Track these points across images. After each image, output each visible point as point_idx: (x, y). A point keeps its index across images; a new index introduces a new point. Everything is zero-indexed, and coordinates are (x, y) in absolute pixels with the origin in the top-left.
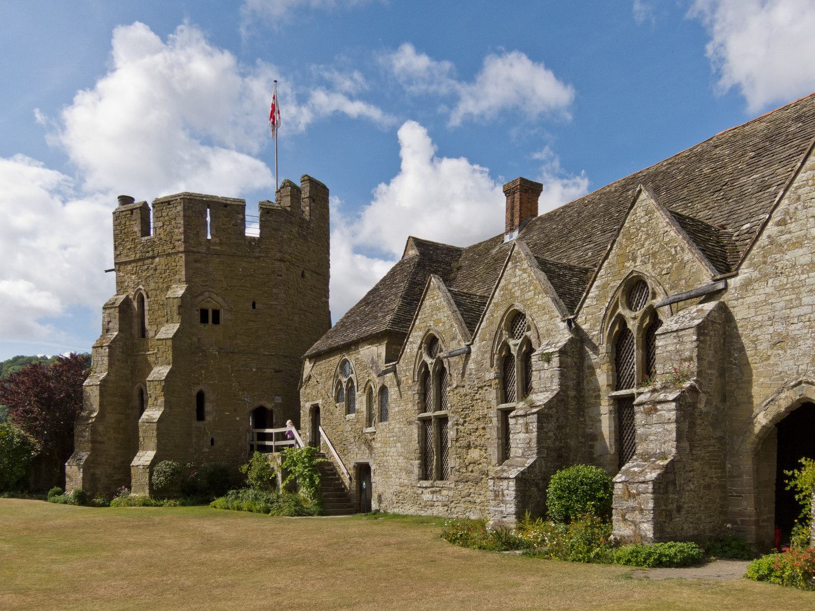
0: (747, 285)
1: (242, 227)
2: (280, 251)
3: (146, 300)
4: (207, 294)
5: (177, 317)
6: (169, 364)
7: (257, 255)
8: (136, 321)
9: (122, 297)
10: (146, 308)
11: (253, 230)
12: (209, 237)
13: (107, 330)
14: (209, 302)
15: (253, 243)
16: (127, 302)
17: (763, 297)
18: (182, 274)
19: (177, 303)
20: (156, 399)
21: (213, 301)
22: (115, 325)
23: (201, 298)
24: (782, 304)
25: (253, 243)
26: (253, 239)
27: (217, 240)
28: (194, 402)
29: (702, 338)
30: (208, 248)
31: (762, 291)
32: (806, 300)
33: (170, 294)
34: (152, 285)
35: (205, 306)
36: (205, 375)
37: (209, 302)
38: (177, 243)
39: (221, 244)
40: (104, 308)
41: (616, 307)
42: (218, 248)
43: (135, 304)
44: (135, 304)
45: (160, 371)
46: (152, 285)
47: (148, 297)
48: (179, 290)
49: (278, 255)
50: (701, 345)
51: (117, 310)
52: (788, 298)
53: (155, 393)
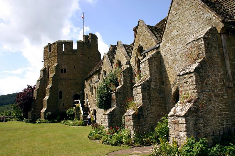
2: (82, 52)
3: (49, 68)
4: (63, 65)
5: (54, 72)
8: (47, 74)
10: (49, 70)
11: (75, 47)
12: (64, 51)
13: (40, 76)
17: (168, 48)
18: (57, 61)
19: (55, 68)
21: (65, 67)
22: (42, 75)
23: (61, 66)
24: (173, 49)
26: (75, 50)
27: (65, 51)
28: (59, 94)
30: (63, 53)
31: (168, 46)
32: (178, 47)
33: (54, 66)
34: (51, 64)
38: (56, 53)
39: (66, 52)
41: (138, 57)
43: (47, 69)
44: (47, 69)
45: (50, 86)
46: (51, 64)
48: (56, 65)
49: (81, 53)
52: (174, 47)
53: (48, 92)
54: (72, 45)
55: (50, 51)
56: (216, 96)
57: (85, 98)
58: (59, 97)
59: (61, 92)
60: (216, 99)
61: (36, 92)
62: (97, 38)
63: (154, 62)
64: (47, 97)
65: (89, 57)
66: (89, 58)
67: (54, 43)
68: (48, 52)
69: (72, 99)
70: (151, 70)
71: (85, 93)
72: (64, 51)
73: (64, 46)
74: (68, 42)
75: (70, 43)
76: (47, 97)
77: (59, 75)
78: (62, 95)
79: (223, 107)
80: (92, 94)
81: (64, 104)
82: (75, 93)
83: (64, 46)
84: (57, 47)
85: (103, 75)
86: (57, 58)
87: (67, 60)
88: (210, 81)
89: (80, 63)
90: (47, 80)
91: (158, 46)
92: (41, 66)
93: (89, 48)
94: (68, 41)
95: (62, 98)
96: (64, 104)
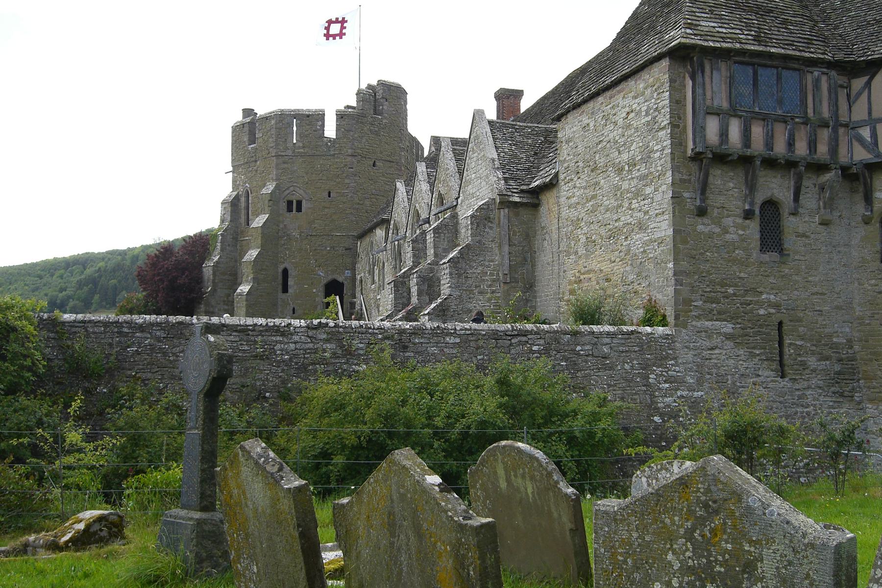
0: (462, 201)
1: (321, 132)
2: (352, 149)
4: (292, 189)
6: (259, 248)
7: (332, 153)
9: (235, 193)
10: (250, 202)
11: (330, 130)
12: (295, 141)
14: (293, 194)
15: (329, 144)
16: (237, 198)
20: (248, 277)
23: (288, 192)
25: (329, 144)
26: (330, 140)
29: (437, 235)
30: (294, 152)
33: (264, 191)
35: (290, 198)
36: (289, 255)
37: (293, 194)
39: (304, 147)
40: (222, 203)
42: (302, 150)
43: (243, 199)
44: (243, 199)
47: (251, 193)
48: (270, 188)
50: (437, 239)
51: (230, 204)
53: (247, 272)
54: (320, 123)
55: (252, 141)
56: (481, 293)
57: (358, 294)
58: (280, 287)
59: (285, 272)
60: (481, 298)
61: (210, 269)
62: (405, 93)
63: (445, 234)
64: (244, 288)
65: (375, 162)
66: (374, 165)
67: (267, 118)
68: (247, 144)
69: (322, 294)
70: (438, 247)
71: (358, 277)
72: (295, 141)
73: (295, 128)
74: (308, 116)
75: (315, 119)
76: (244, 288)
77: (281, 219)
78: (291, 282)
79: (492, 307)
80: (373, 282)
81: (294, 309)
82: (330, 278)
83: (295, 128)
84: (273, 131)
85: (393, 233)
86: (274, 165)
87: (307, 173)
88: (475, 273)
89: (347, 181)
90: (242, 232)
91: (455, 204)
92: (225, 188)
93: (377, 134)
94: (309, 111)
95: (290, 290)
96: (294, 309)
